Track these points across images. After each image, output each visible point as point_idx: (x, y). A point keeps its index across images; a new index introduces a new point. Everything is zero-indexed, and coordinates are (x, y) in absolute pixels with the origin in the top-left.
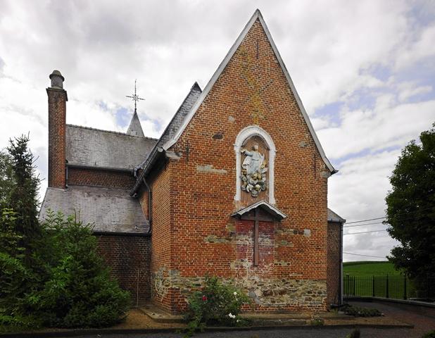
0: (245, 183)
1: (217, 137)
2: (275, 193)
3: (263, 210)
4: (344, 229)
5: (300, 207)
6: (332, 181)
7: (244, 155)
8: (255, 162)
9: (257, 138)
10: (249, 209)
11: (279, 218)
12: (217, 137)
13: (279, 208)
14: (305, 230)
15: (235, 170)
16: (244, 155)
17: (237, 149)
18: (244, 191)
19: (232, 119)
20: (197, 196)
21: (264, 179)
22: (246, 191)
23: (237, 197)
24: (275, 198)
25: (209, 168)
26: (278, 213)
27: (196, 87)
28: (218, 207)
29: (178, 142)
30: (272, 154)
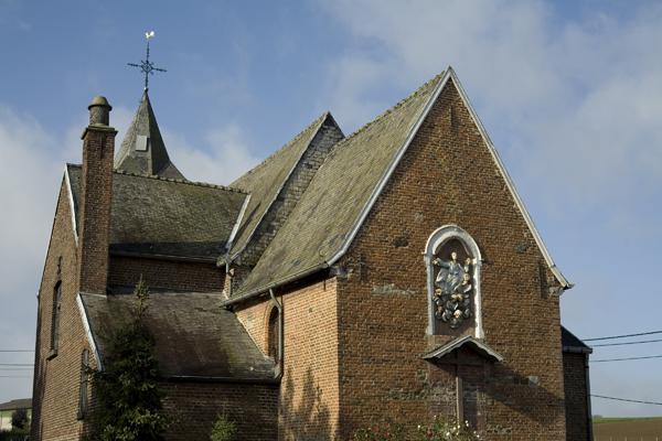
0: (440, 309)
2: (483, 322)
3: (469, 347)
4: (590, 364)
5: (520, 343)
6: (565, 300)
8: (453, 277)
9: (454, 244)
10: (448, 348)
11: (492, 360)
13: (491, 344)
14: (530, 378)
16: (437, 268)
17: (427, 260)
18: (438, 319)
19: (417, 217)
20: (377, 330)
21: (467, 301)
22: (441, 319)
23: (429, 331)
25: (390, 288)
26: (490, 352)
27: (329, 121)
29: (348, 253)
30: (477, 260)
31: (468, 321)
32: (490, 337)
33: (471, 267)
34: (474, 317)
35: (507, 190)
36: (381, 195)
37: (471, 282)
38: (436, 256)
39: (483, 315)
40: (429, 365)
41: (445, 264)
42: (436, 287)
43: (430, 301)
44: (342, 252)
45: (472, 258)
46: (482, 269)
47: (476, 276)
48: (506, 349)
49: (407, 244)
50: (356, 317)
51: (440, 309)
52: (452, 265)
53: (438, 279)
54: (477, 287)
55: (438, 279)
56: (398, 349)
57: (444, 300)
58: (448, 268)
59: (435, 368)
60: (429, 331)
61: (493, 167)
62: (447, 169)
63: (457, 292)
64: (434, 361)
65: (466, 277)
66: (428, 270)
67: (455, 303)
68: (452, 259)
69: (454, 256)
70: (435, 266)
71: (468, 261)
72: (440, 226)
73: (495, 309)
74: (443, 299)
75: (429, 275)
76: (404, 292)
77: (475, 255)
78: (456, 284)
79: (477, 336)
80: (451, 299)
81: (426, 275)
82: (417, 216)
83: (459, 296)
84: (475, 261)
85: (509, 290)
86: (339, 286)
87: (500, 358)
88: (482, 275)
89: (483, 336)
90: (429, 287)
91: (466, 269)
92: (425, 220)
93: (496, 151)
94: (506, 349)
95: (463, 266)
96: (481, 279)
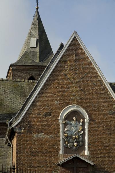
1: (46, 115)
7: (65, 125)
8: (74, 128)
9: (74, 113)
12: (46, 115)
15: (60, 135)
16: (65, 125)
17: (60, 122)
18: (65, 147)
20: (34, 153)
21: (81, 139)
22: (67, 147)
23: (61, 152)
24: (89, 150)
25: (42, 135)
26: (87, 161)
28: (48, 159)
29: (21, 121)
31: (81, 147)
32: (93, 155)
33: (84, 123)
34: (85, 145)
35: (105, 86)
36: (38, 95)
37: (83, 129)
38: (65, 119)
39: (89, 144)
40: (60, 168)
41: (69, 122)
42: (65, 133)
43: (61, 140)
44: (19, 121)
45: (84, 119)
46: (89, 123)
47: (86, 127)
48: (101, 159)
49: (50, 115)
50: (25, 149)
51: (66, 142)
52: (73, 123)
53: (66, 130)
54: (86, 132)
55: (66, 130)
56: (45, 161)
57: (69, 138)
58: (71, 124)
59: (63, 169)
60: (61, 152)
61: (97, 75)
62: (72, 80)
63: (76, 134)
64: (58, 165)
65: (80, 128)
66: (61, 126)
67: (75, 140)
68: (74, 120)
69: (74, 118)
70: (64, 124)
71: (82, 120)
72: (67, 106)
73: (96, 141)
74: (68, 138)
75: (61, 128)
76: (48, 136)
77: (86, 118)
78: (75, 131)
79: (86, 154)
80: (72, 138)
81: (59, 128)
82: (56, 102)
83: (77, 136)
84: (86, 120)
85: (103, 133)
86: (18, 136)
87: (92, 164)
88: (89, 126)
89: (89, 153)
90: (61, 133)
91: (81, 124)
92: (60, 104)
93: (99, 68)
94: (101, 159)
95: (80, 123)
96: (88, 128)
